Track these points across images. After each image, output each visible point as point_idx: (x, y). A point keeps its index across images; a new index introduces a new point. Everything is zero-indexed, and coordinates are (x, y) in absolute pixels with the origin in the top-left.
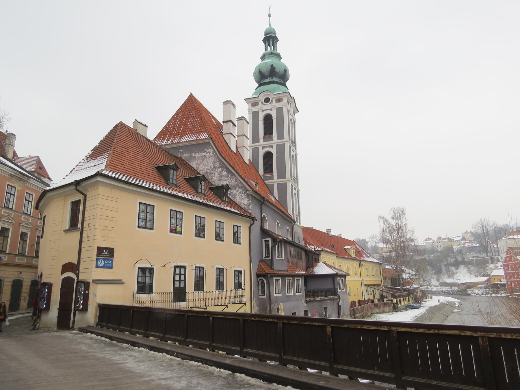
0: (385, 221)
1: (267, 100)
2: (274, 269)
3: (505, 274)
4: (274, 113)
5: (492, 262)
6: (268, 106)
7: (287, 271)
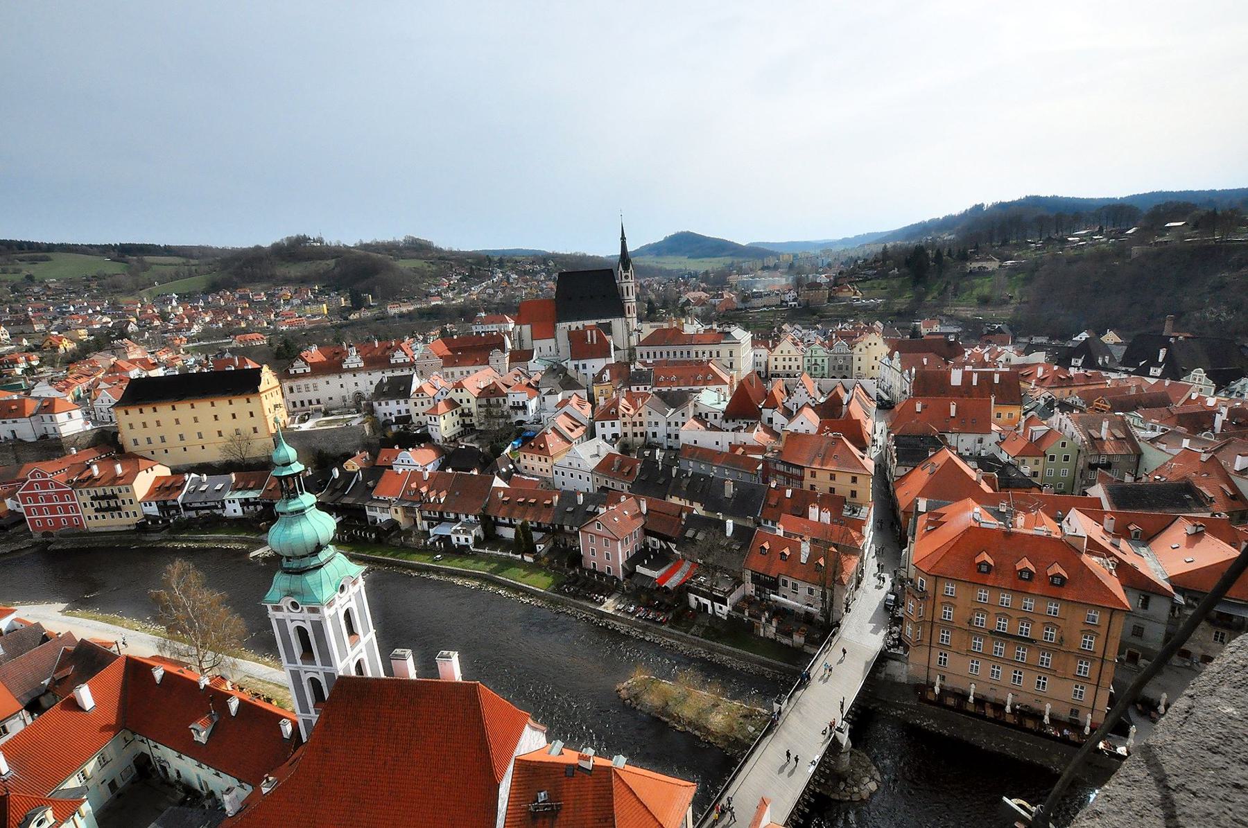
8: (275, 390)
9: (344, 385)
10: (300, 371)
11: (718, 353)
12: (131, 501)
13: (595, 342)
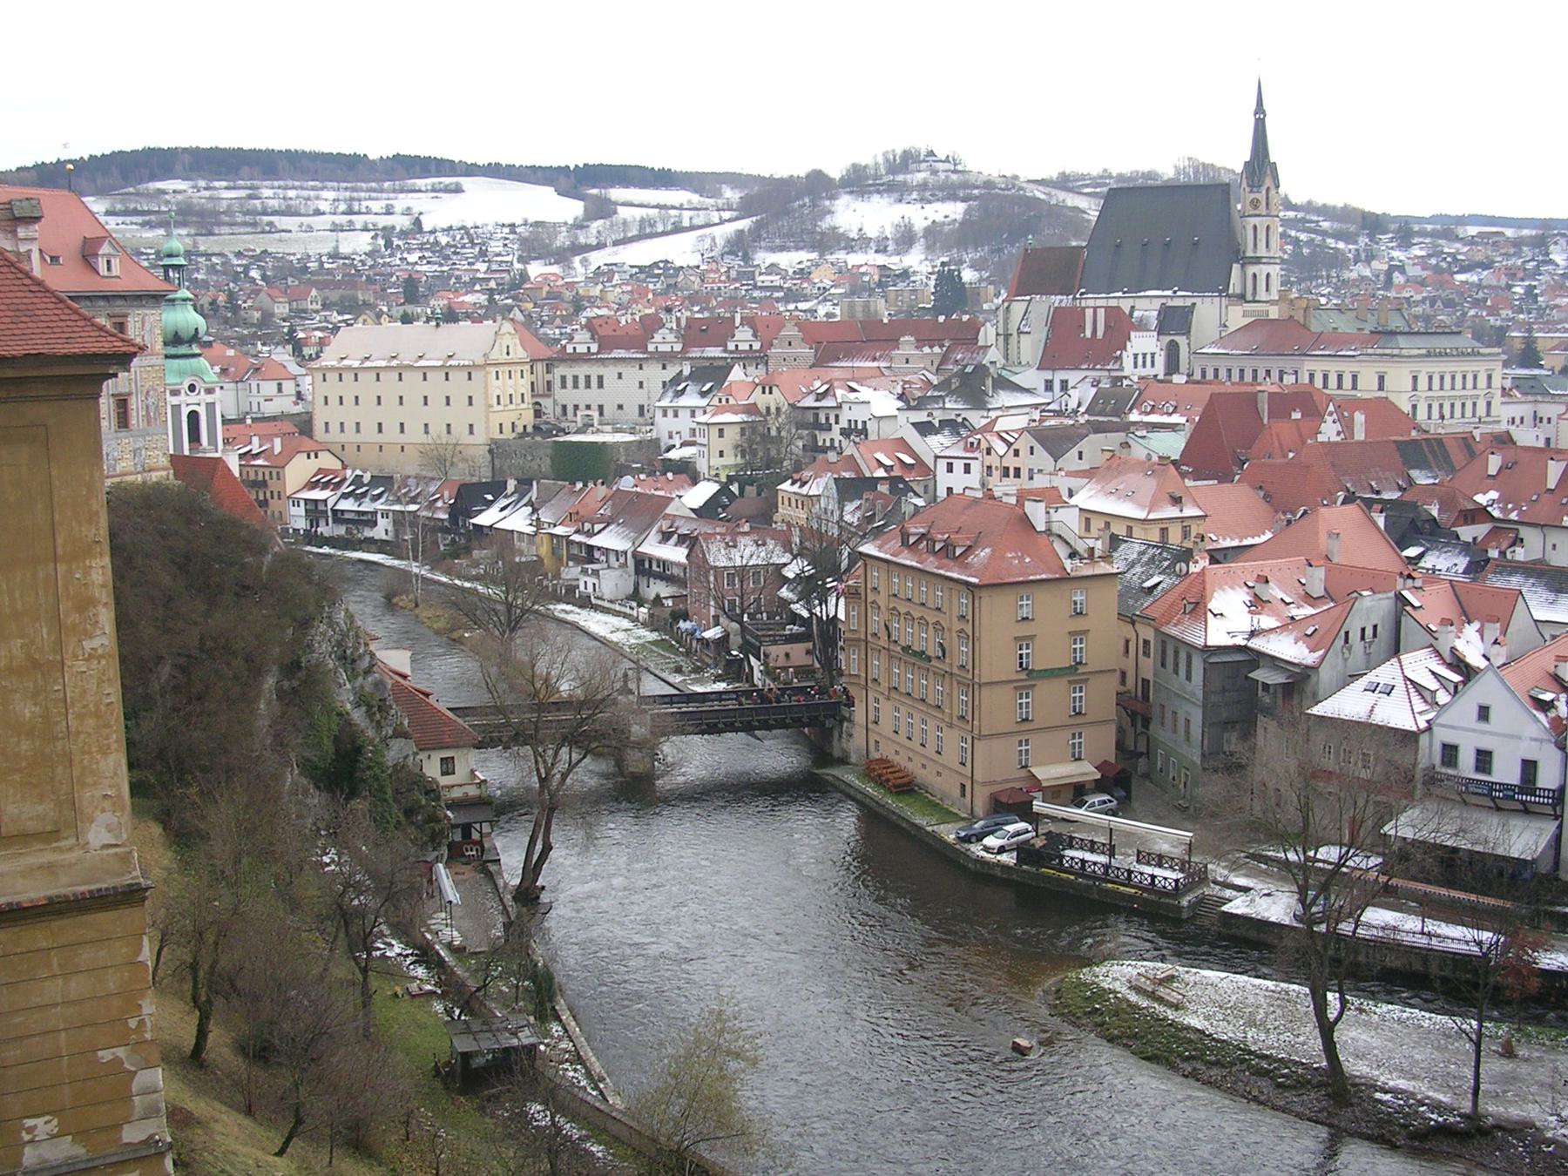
1: (192, 388)
4: (202, 411)
6: (193, 398)
8: (519, 368)
9: (645, 384)
10: (582, 349)
11: (1355, 378)
13: (1100, 334)
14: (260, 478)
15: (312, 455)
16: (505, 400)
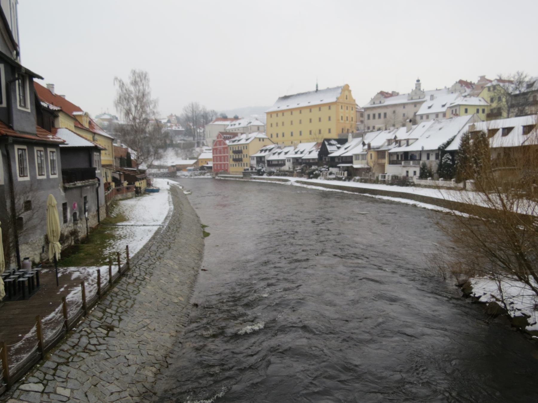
0: (122, 85)
2: (15, 128)
3: (214, 157)
5: (198, 146)
7: (36, 135)
12: (247, 155)
14: (240, 149)
15: (261, 140)
16: (345, 118)
